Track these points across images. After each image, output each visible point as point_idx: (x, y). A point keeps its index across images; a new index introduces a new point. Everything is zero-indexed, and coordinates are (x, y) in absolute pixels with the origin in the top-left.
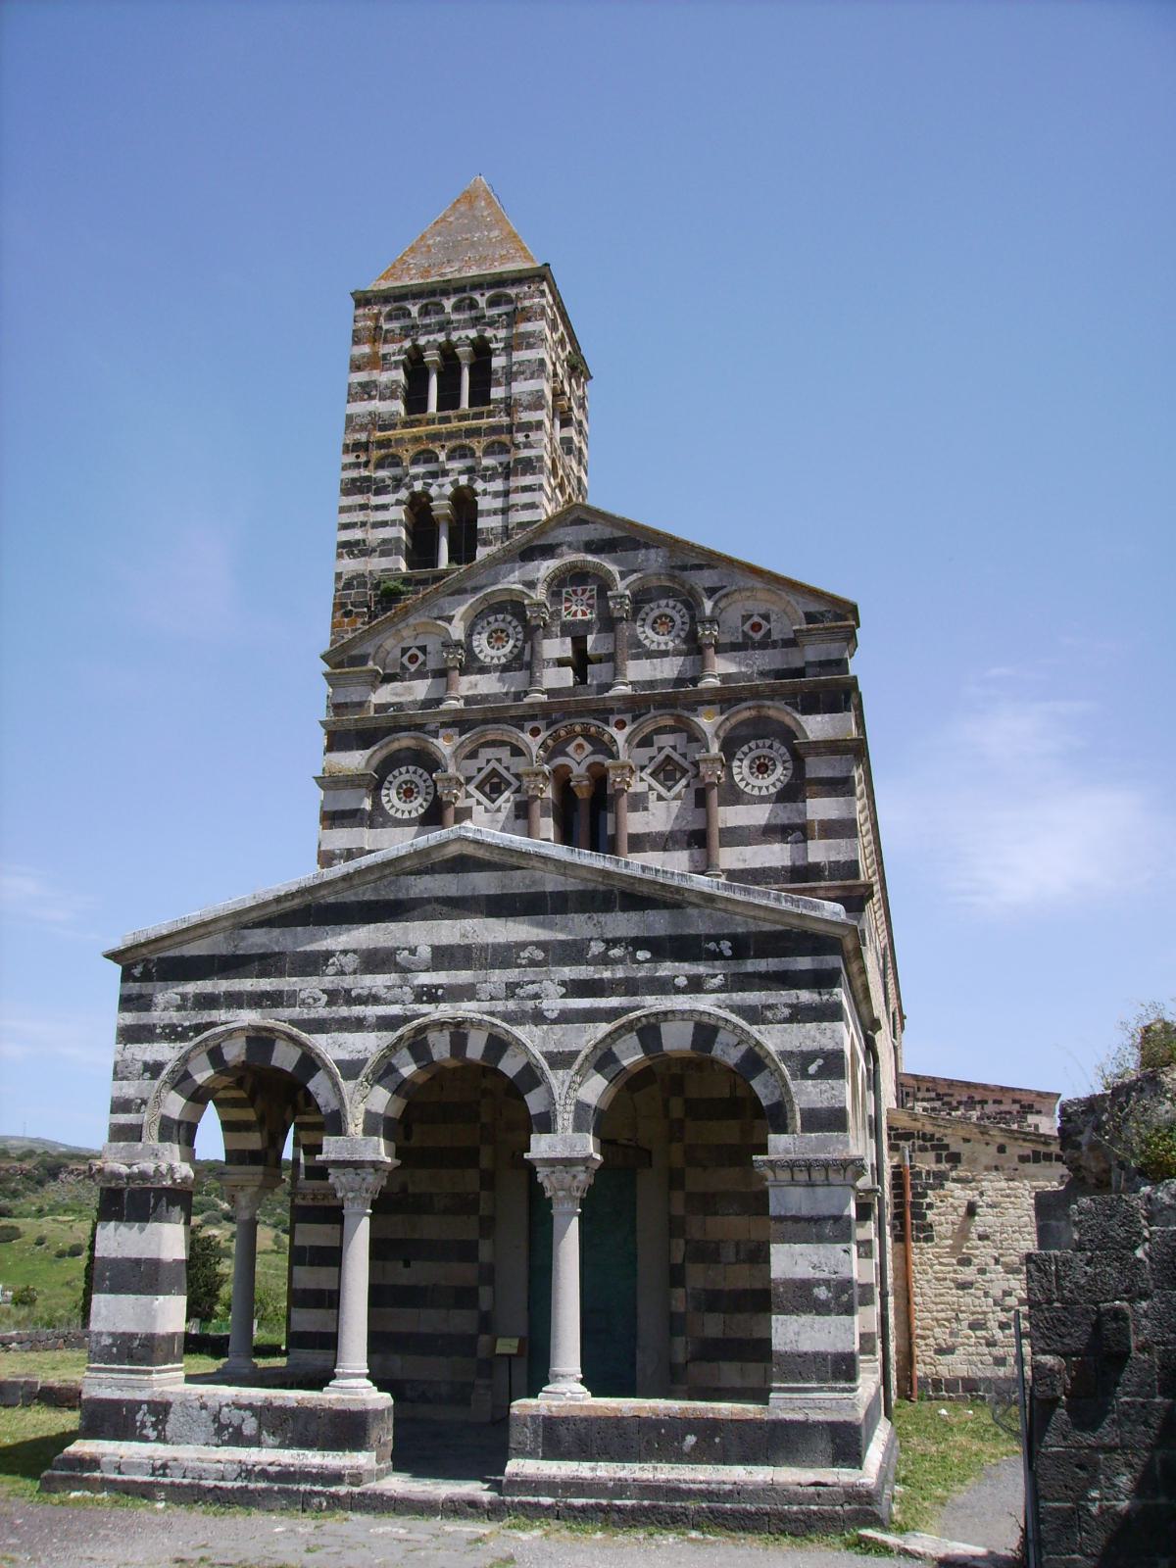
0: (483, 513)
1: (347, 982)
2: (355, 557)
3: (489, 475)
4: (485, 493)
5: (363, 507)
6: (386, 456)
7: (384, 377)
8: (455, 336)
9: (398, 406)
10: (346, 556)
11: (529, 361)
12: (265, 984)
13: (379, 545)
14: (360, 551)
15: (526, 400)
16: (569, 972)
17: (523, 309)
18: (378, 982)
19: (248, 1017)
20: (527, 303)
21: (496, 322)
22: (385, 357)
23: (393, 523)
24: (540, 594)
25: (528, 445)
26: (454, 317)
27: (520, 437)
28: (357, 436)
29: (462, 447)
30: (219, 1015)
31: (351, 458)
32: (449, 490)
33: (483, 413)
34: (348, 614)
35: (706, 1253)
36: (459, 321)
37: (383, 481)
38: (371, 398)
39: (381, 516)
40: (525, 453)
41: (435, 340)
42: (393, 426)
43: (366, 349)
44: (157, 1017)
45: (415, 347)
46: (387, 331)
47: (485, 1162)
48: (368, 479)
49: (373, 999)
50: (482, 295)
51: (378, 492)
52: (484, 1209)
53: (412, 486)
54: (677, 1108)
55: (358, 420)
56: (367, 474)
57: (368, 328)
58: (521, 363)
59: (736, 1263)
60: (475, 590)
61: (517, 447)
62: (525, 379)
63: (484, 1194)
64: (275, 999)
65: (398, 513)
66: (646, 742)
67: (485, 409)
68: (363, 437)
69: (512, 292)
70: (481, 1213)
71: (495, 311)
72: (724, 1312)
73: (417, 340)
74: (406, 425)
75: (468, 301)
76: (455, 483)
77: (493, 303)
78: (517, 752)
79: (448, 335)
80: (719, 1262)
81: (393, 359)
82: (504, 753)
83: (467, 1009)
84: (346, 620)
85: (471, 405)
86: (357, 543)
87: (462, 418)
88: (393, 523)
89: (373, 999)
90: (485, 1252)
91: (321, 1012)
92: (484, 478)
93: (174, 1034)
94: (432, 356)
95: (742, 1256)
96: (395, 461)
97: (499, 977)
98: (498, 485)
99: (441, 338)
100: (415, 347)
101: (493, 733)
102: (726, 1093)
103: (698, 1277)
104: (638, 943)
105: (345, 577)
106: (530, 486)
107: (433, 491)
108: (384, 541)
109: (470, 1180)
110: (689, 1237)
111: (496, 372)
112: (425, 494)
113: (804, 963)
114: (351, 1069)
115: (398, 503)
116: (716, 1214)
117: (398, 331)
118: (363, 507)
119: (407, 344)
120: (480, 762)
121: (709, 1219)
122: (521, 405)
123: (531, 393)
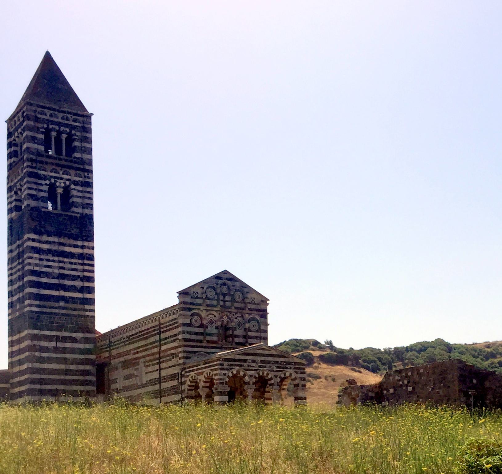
0: (73, 196)
1: (250, 364)
3: (76, 183)
4: (75, 189)
12: (239, 363)
16: (277, 365)
18: (254, 364)
19: (238, 368)
24: (219, 286)
30: (234, 367)
32: (63, 185)
44: (225, 367)
49: (254, 367)
58: (85, 147)
60: (208, 283)
64: (241, 366)
66: (236, 318)
69: (81, 119)
76: (65, 183)
77: (74, 121)
78: (215, 316)
82: (213, 316)
83: (265, 369)
85: (66, 156)
87: (66, 160)
89: (254, 367)
91: (247, 368)
93: (227, 370)
97: (268, 365)
98: (79, 188)
101: (212, 312)
104: (285, 362)
111: (75, 147)
113: (302, 367)
114: (251, 376)
120: (209, 317)
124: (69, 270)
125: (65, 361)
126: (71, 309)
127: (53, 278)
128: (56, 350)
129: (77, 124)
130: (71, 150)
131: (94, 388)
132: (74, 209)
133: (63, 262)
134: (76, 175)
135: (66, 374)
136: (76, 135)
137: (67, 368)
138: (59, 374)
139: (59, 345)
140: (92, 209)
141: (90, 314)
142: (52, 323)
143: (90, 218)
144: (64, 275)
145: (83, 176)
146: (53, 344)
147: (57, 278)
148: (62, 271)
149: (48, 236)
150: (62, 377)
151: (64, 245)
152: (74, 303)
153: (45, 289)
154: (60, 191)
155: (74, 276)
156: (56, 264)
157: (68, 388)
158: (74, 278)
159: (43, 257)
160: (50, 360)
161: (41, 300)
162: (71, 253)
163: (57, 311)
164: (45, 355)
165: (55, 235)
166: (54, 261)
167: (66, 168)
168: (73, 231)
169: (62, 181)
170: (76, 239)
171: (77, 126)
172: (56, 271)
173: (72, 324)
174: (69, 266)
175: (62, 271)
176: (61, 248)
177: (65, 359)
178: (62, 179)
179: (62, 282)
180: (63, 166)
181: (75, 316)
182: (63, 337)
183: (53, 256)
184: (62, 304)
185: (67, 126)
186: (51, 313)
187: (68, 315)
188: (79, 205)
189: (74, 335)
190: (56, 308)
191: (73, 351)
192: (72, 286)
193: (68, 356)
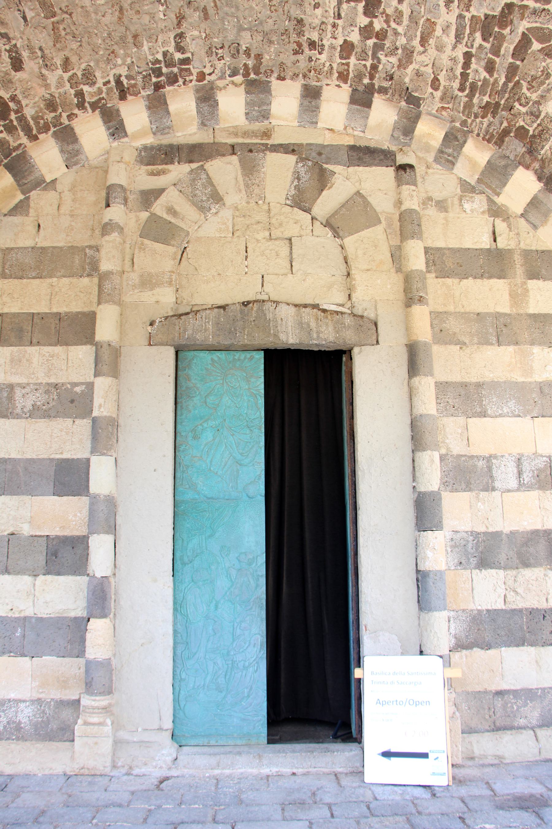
35: (470, 474)
47: (106, 330)
52: (102, 407)
54: (416, 260)
59: (518, 490)
63: (102, 384)
70: (95, 413)
72: (505, 568)
80: (494, 489)
90: (102, 477)
95: (527, 477)
102: (485, 242)
103: (462, 513)
109: (74, 363)
110: (443, 451)
116: (483, 414)
121: (474, 422)
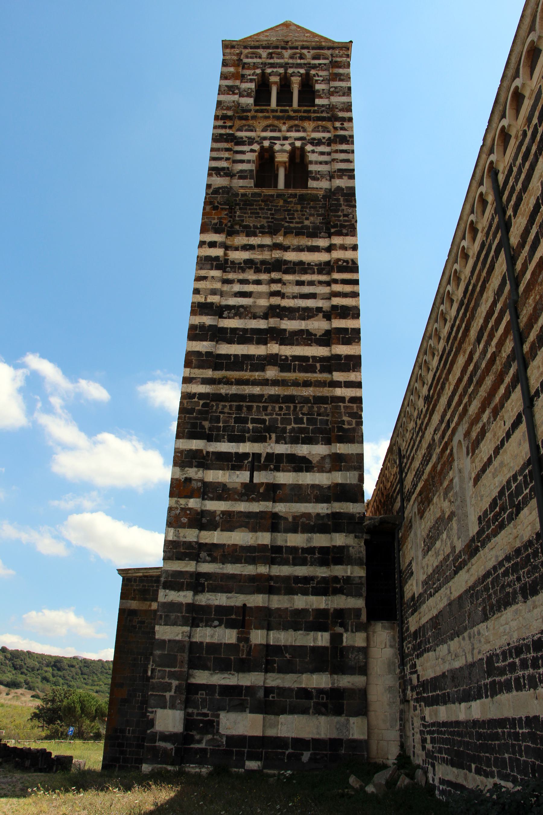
0: (311, 162)
2: (221, 176)
4: (313, 152)
5: (227, 150)
6: (245, 125)
7: (245, 86)
8: (290, 71)
9: (251, 101)
10: (214, 175)
11: (341, 87)
13: (238, 173)
14: (224, 173)
15: (340, 106)
17: (336, 62)
20: (338, 59)
21: (317, 67)
22: (243, 76)
23: (249, 162)
25: (343, 129)
26: (291, 61)
27: (338, 124)
28: (225, 112)
29: (296, 126)
31: (220, 123)
32: (288, 148)
33: (311, 110)
34: (215, 208)
36: (293, 64)
37: (242, 138)
38: (234, 94)
39: (239, 157)
40: (342, 133)
41: (277, 71)
42: (250, 111)
43: (232, 69)
45: (263, 73)
46: (245, 63)
48: (233, 135)
50: (309, 52)
51: (240, 142)
53: (262, 143)
55: (226, 104)
56: (231, 132)
57: (234, 60)
58: (336, 88)
61: (336, 129)
62: (339, 96)
65: (252, 156)
67: (312, 109)
68: (230, 113)
69: (328, 52)
71: (317, 62)
73: (265, 70)
74: (257, 111)
75: (298, 55)
77: (316, 57)
79: (286, 70)
81: (249, 77)
84: (214, 212)
86: (223, 169)
88: (249, 162)
92: (312, 144)
94: (274, 79)
96: (251, 129)
99: (282, 71)
100: (263, 73)
105: (212, 188)
106: (346, 150)
107: (277, 147)
108: (241, 171)
111: (318, 91)
112: (271, 148)
115: (252, 151)
117: (252, 64)
118: (227, 150)
119: (258, 71)
122: (337, 108)
123: (344, 103)
124: (294, 297)
125: (273, 523)
126: (296, 384)
127: (255, 317)
128: (249, 491)
129: (321, 61)
130: (308, 92)
131: (359, 603)
132: (312, 184)
133: (279, 281)
134: (316, 129)
135: (273, 562)
136: (318, 76)
137: (280, 543)
138: (253, 561)
139: (260, 477)
140: (352, 177)
141: (349, 393)
142: (245, 421)
143: (350, 195)
144: (285, 309)
145: (331, 128)
146: (243, 477)
147: (265, 316)
148: (276, 301)
149: (247, 235)
150: (263, 569)
151: (286, 249)
152: (312, 369)
153: (230, 342)
154: (282, 158)
155: (307, 309)
156: (263, 288)
157: (278, 602)
158: (307, 314)
159: (231, 276)
160: (230, 521)
161: (216, 367)
162: (301, 263)
163: (257, 390)
164: (217, 506)
165: (263, 233)
166: (258, 282)
167: (297, 121)
168: (307, 223)
169: (285, 142)
170: (313, 235)
171: (320, 64)
172: (263, 302)
173: (299, 421)
174: (297, 290)
175: (276, 301)
176: (277, 254)
177: (275, 516)
178: (286, 138)
179: (273, 322)
180: (290, 118)
181: (306, 400)
182: (270, 456)
183: (258, 271)
184: (271, 373)
185: (299, 66)
186: (241, 398)
187: (290, 399)
188: (323, 177)
189: (302, 450)
190: (255, 383)
191: (298, 494)
192: (302, 331)
193: (281, 508)
